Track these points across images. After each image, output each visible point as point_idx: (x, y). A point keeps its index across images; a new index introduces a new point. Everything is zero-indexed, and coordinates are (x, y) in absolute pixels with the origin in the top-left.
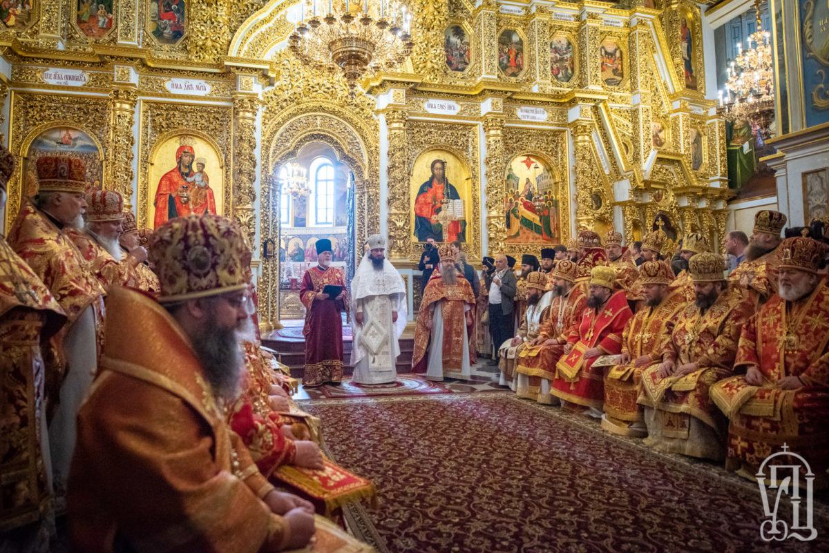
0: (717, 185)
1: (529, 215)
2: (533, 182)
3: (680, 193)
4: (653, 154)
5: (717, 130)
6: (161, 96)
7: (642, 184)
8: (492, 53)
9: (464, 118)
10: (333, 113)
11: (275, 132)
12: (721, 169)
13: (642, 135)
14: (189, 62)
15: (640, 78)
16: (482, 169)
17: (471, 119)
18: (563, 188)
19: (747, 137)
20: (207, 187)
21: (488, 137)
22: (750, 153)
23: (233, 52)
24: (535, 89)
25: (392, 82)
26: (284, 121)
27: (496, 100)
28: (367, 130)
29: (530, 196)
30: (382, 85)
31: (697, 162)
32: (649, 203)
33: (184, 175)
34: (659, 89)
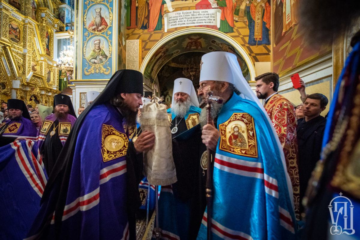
0: (55, 89)
3: (42, 89)
4: (31, 73)
5: (56, 71)
7: (26, 83)
12: (57, 84)
13: (27, 65)
15: (28, 44)
19: (66, 76)
22: (66, 81)
31: (49, 80)
32: (29, 91)
34: (36, 50)
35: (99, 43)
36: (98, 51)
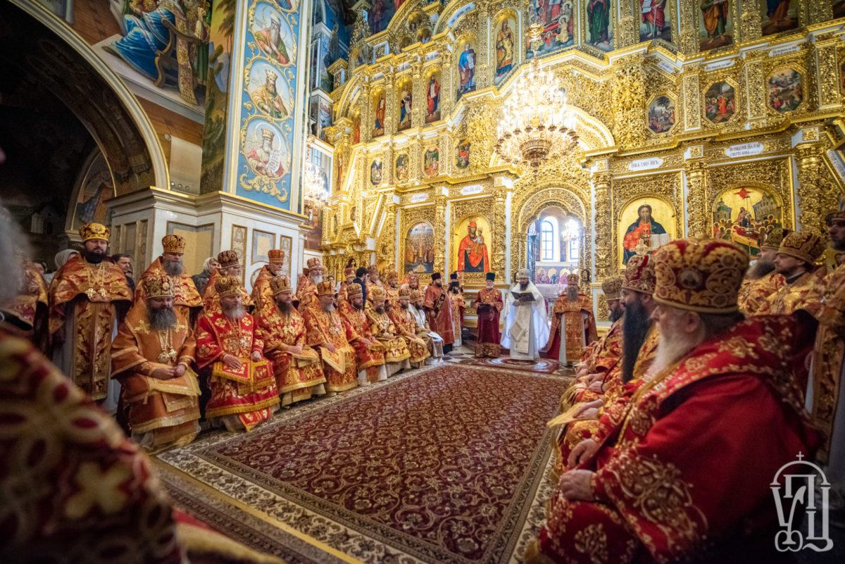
2: (751, 211)
6: (457, 198)
8: (695, 108)
9: (666, 169)
10: (559, 186)
11: (522, 206)
14: (472, 176)
16: (684, 206)
17: (674, 168)
18: (786, 211)
20: (483, 244)
21: (689, 179)
23: (491, 166)
24: (747, 127)
25: (595, 157)
26: (527, 198)
27: (695, 147)
28: (584, 192)
29: (745, 223)
30: (589, 161)
33: (472, 238)
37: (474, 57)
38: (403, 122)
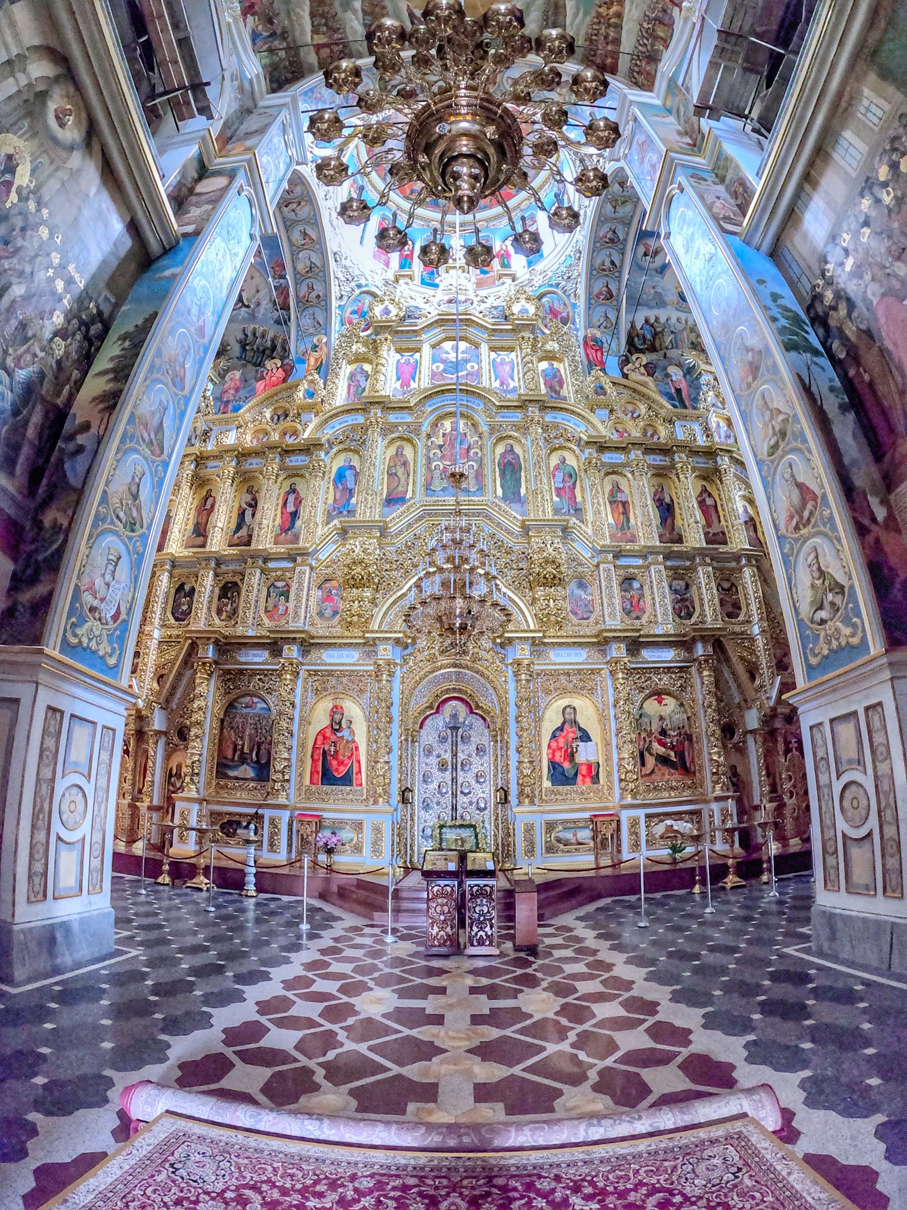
1: (661, 750)
10: (467, 667)
20: (354, 741)
35: (817, 557)
36: (821, 581)
37: (357, 474)
38: (239, 534)
